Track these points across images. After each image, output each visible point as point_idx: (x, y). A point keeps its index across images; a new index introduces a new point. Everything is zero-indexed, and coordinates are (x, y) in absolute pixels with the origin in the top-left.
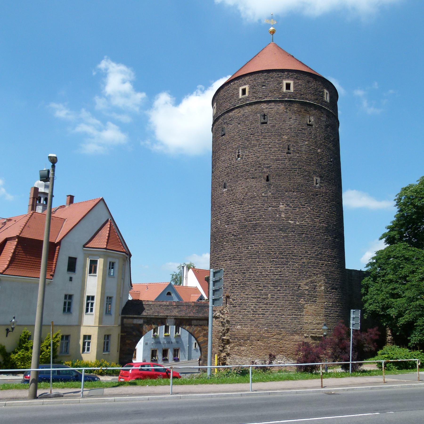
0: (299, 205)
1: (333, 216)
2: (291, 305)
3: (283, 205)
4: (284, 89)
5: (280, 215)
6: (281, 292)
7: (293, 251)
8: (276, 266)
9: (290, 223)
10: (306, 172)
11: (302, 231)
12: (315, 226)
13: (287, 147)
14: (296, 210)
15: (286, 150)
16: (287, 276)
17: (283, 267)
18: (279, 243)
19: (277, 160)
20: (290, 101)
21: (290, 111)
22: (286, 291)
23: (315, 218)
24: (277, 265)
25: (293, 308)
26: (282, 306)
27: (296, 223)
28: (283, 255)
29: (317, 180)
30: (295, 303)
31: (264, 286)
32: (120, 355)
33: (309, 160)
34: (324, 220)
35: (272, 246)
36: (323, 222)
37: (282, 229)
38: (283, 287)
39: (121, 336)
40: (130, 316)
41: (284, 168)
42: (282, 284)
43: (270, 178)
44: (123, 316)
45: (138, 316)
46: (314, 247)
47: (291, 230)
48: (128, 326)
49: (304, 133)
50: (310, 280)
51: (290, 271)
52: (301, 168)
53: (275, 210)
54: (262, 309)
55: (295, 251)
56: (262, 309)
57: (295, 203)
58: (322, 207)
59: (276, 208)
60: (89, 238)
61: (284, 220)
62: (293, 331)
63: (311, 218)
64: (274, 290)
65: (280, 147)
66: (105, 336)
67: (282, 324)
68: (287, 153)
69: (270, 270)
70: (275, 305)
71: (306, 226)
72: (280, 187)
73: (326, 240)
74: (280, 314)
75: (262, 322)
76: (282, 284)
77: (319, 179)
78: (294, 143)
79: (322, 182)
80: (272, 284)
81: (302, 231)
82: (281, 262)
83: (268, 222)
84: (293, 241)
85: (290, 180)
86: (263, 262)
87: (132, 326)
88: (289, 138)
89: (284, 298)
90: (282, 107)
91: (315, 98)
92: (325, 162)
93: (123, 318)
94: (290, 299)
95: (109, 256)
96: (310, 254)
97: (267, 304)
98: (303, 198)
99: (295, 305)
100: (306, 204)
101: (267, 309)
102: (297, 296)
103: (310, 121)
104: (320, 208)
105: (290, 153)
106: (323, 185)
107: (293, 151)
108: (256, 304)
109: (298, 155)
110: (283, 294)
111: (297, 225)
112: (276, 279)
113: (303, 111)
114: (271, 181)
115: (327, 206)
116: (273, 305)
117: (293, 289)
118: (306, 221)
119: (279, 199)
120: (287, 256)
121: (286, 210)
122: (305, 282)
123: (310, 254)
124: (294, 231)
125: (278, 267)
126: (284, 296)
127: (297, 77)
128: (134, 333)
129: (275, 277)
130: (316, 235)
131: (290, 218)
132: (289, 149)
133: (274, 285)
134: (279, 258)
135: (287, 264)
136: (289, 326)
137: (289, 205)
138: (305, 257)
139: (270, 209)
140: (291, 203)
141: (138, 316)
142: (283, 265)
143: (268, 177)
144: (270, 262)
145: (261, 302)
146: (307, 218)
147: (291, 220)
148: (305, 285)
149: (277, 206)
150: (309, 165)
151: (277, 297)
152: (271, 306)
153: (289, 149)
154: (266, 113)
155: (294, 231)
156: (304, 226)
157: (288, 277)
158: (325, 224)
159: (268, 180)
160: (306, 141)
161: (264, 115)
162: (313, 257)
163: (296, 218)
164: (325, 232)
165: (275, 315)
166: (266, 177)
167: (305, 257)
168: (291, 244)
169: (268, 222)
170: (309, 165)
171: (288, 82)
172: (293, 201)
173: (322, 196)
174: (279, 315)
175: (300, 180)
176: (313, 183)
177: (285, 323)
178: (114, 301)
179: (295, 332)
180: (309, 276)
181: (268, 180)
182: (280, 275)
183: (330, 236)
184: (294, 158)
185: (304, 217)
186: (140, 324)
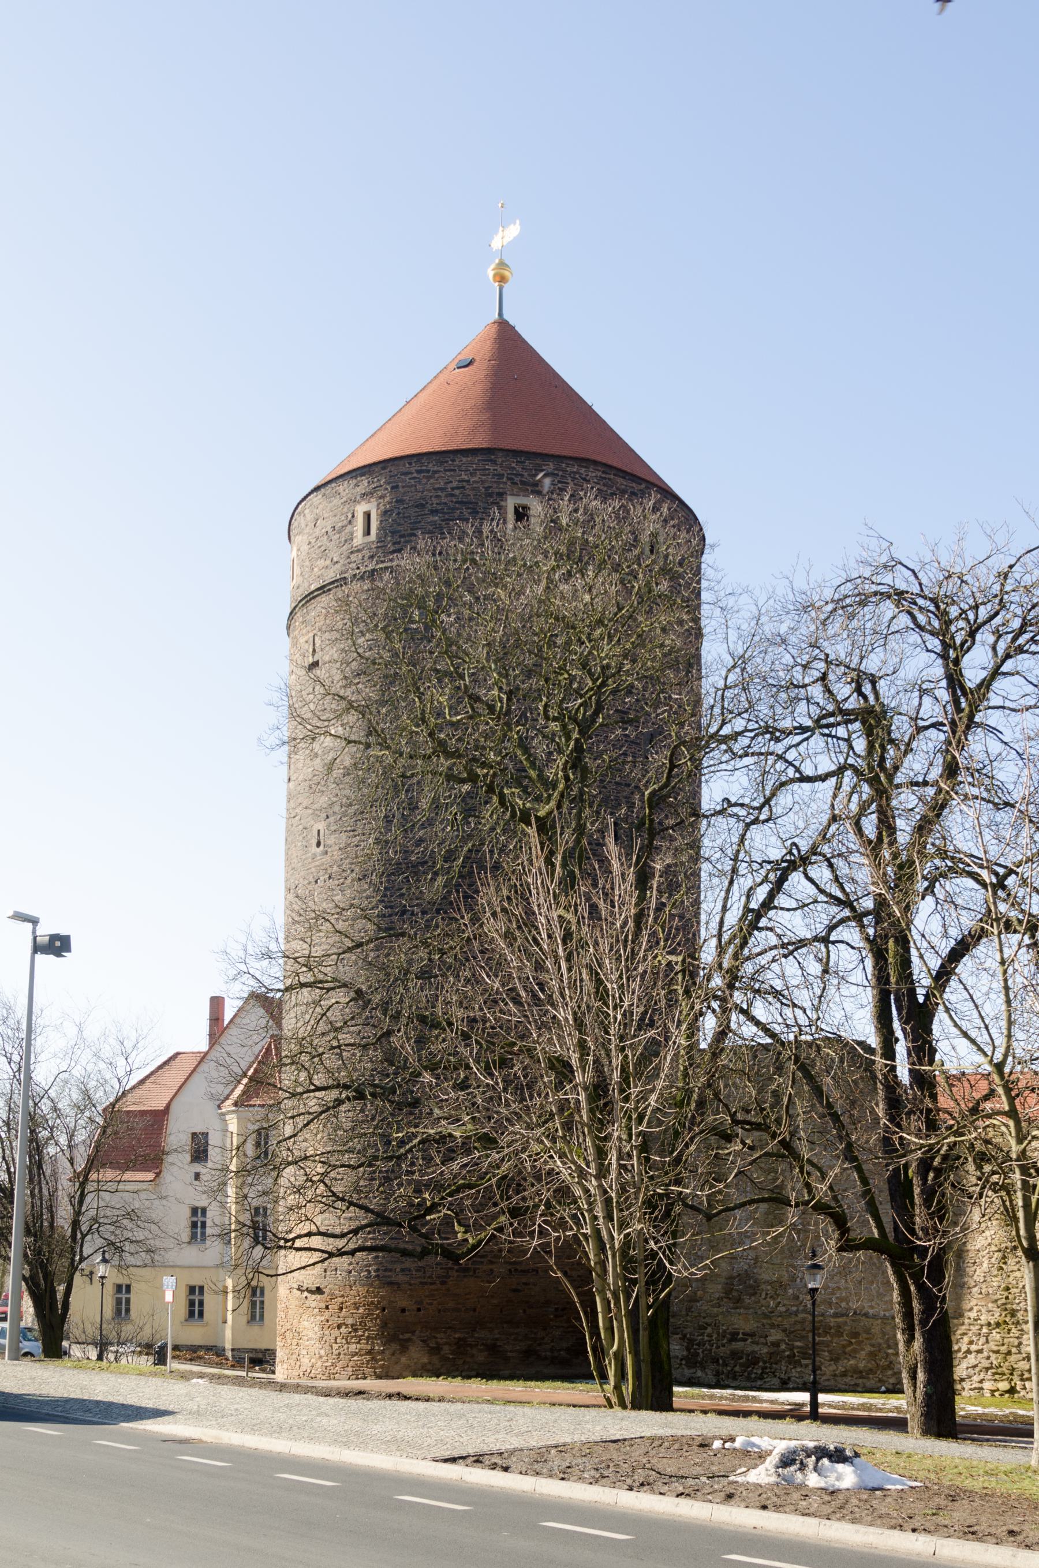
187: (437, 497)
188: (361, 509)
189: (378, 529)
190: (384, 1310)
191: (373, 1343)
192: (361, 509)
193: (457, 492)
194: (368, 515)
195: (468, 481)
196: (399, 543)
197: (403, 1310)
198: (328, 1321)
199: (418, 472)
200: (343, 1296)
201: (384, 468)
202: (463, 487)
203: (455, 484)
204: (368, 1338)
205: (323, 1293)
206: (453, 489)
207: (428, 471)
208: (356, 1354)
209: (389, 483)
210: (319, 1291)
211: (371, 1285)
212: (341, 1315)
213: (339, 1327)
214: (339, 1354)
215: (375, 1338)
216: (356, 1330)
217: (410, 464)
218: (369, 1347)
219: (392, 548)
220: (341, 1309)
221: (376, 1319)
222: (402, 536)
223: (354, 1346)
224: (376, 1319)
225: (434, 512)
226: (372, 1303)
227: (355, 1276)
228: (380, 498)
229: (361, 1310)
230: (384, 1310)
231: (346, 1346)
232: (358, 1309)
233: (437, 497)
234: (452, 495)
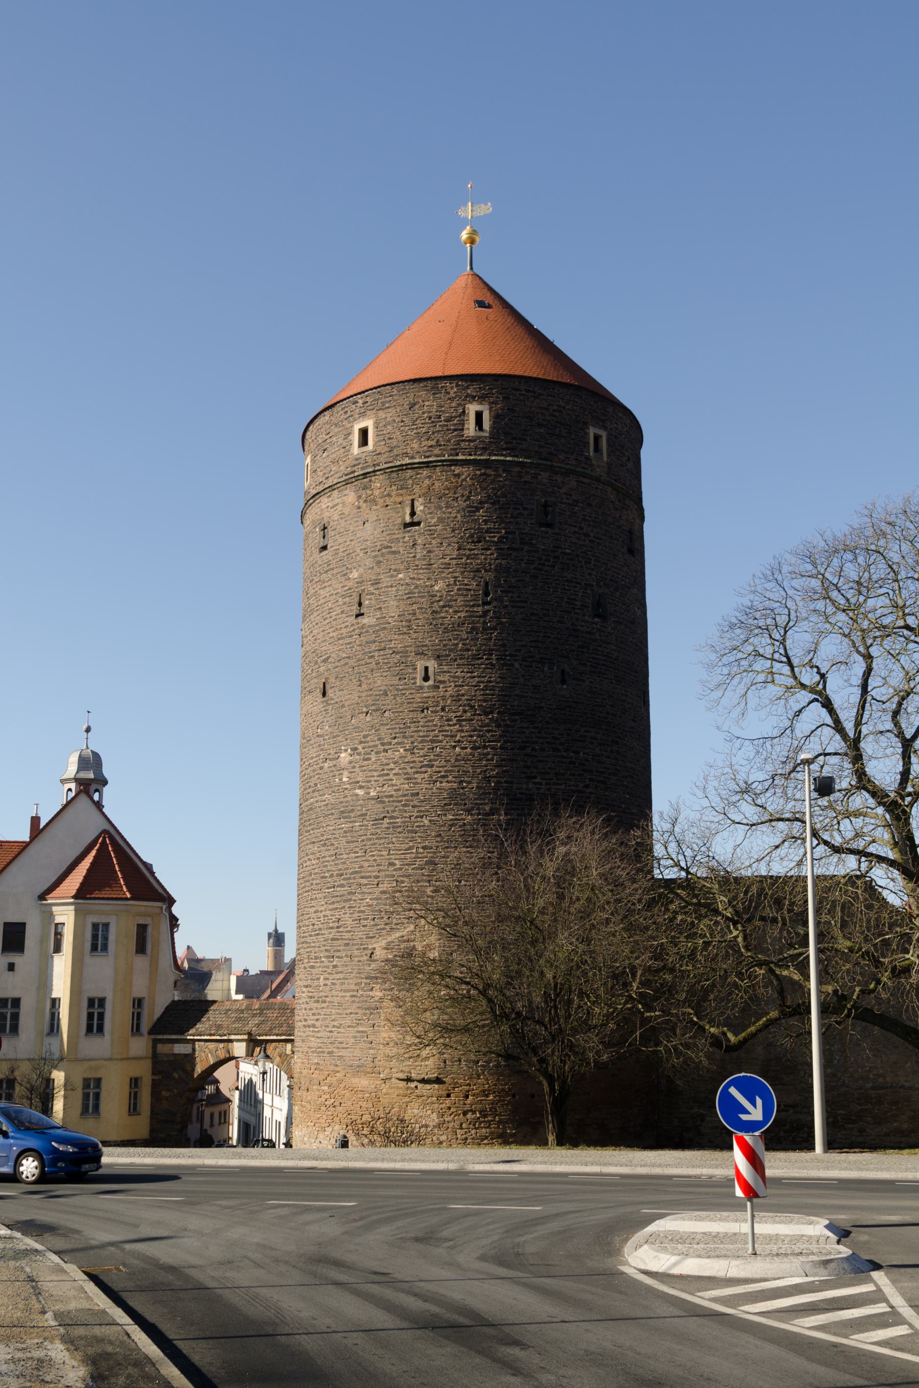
0: (376, 746)
1: (488, 754)
2: (354, 1002)
3: (346, 750)
4: (356, 450)
5: (341, 780)
6: (339, 970)
7: (362, 867)
8: (333, 906)
9: (357, 795)
10: (397, 653)
11: (383, 812)
12: (418, 794)
13: (357, 600)
14: (369, 759)
15: (355, 609)
16: (349, 929)
17: (344, 907)
18: (337, 848)
19: (339, 639)
20: (365, 475)
21: (365, 501)
22: (347, 966)
23: (417, 772)
24: (333, 903)
25: (358, 1008)
26: (340, 1004)
27: (369, 793)
28: (344, 879)
29: (426, 668)
30: (362, 995)
31: (316, 958)
32: (151, 1125)
33: (406, 621)
34: (445, 771)
35: (327, 859)
36: (442, 777)
37: (342, 812)
38: (342, 957)
39: (153, 1080)
40: (165, 1037)
41: (349, 658)
42: (339, 951)
43: (328, 687)
44: (153, 1037)
45: (179, 1037)
46: (410, 848)
47: (359, 813)
48: (165, 1059)
49: (394, 553)
50: (398, 934)
51: (356, 915)
52: (384, 649)
53: (335, 766)
54: (314, 1014)
55: (366, 864)
56: (314, 1014)
57: (368, 742)
58: (440, 738)
59: (334, 762)
60: (53, 879)
61: (346, 789)
62: (359, 1066)
63: (405, 774)
64: (328, 967)
65: (344, 604)
66: (131, 1079)
67: (338, 1048)
68: (357, 616)
69: (324, 916)
70: (330, 1002)
71: (391, 796)
72: (343, 706)
73: (451, 826)
74: (336, 1023)
75: (312, 1045)
76: (339, 951)
77: (432, 664)
78: (372, 584)
79: (446, 668)
80: (326, 950)
81: (383, 812)
82: (341, 896)
83: (324, 798)
84: (363, 841)
85: (360, 685)
86: (316, 899)
87: (172, 1058)
88: (361, 576)
89: (342, 984)
90: (350, 496)
91: (433, 443)
92: (456, 612)
93: (155, 1042)
94: (353, 987)
95: (90, 912)
96: (401, 869)
97: (318, 1002)
98: (387, 724)
99: (363, 1002)
100: (395, 738)
101: (319, 1014)
102: (366, 978)
103: (413, 514)
104: (432, 741)
105: (363, 614)
106: (446, 677)
107: (369, 607)
108: (307, 1003)
109: (378, 615)
110: (341, 976)
111: (373, 799)
112: (333, 939)
113: (393, 494)
114: (330, 692)
115: (462, 731)
116: (325, 1002)
117: (359, 961)
118: (393, 785)
119: (340, 738)
120: (350, 878)
121: (351, 762)
122: (383, 943)
123: (401, 869)
124: (366, 815)
125: (336, 909)
126: (344, 979)
127: (383, 403)
128: (176, 1075)
129: (330, 933)
130: (417, 817)
131: (358, 782)
132: (360, 604)
133: (327, 954)
134: (338, 886)
135: (350, 900)
136: (350, 1052)
137: (356, 749)
138: (387, 876)
139: (326, 765)
140: (361, 742)
141: (179, 1037)
142: (345, 901)
143: (324, 684)
144: (325, 897)
145: (311, 997)
146: (395, 774)
147: (361, 787)
148: (384, 948)
149: (336, 756)
150: (405, 633)
151: (333, 984)
152: (324, 1005)
153: (360, 604)
154: (325, 521)
155: (366, 815)
156: (386, 797)
157: (350, 931)
158: (447, 782)
159: (324, 694)
160: (398, 571)
161: (325, 528)
162: (408, 876)
163: (370, 781)
164: (445, 804)
165: (327, 1026)
166: (322, 686)
167: (387, 876)
168: (357, 849)
169: (324, 798)
170: (405, 633)
171: (362, 425)
172: (365, 737)
173: (443, 709)
174: (334, 1026)
175: (380, 681)
176: (415, 678)
177: (344, 1045)
178: (108, 1005)
179: (359, 1070)
180: (396, 924)
181: (324, 694)
182: (338, 927)
183: (469, 811)
184: (369, 626)
185: (388, 775)
186: (186, 1055)
187: (542, 414)
188: (472, 408)
189: (490, 428)
190: (514, 1096)
191: (504, 1127)
192: (472, 408)
193: (557, 414)
194: (479, 415)
195: (564, 408)
196: (511, 443)
197: (533, 1096)
198: (449, 1108)
199: (527, 391)
200: (469, 1085)
201: (496, 380)
202: (561, 411)
203: (555, 407)
204: (499, 1122)
205: (444, 1083)
206: (554, 411)
207: (535, 393)
208: (486, 1138)
209: (501, 394)
210: (438, 1081)
211: (502, 1074)
212: (468, 1101)
213: (465, 1113)
214: (466, 1139)
215: (507, 1123)
216: (485, 1116)
217: (520, 383)
218: (501, 1131)
219: (505, 446)
220: (467, 1097)
221: (507, 1105)
222: (513, 438)
223: (484, 1130)
224: (507, 1105)
225: (540, 425)
226: (503, 1090)
227: (482, 1066)
228: (492, 403)
229: (491, 1097)
230: (514, 1096)
231: (473, 1132)
232: (487, 1096)
233: (542, 414)
234: (553, 416)
